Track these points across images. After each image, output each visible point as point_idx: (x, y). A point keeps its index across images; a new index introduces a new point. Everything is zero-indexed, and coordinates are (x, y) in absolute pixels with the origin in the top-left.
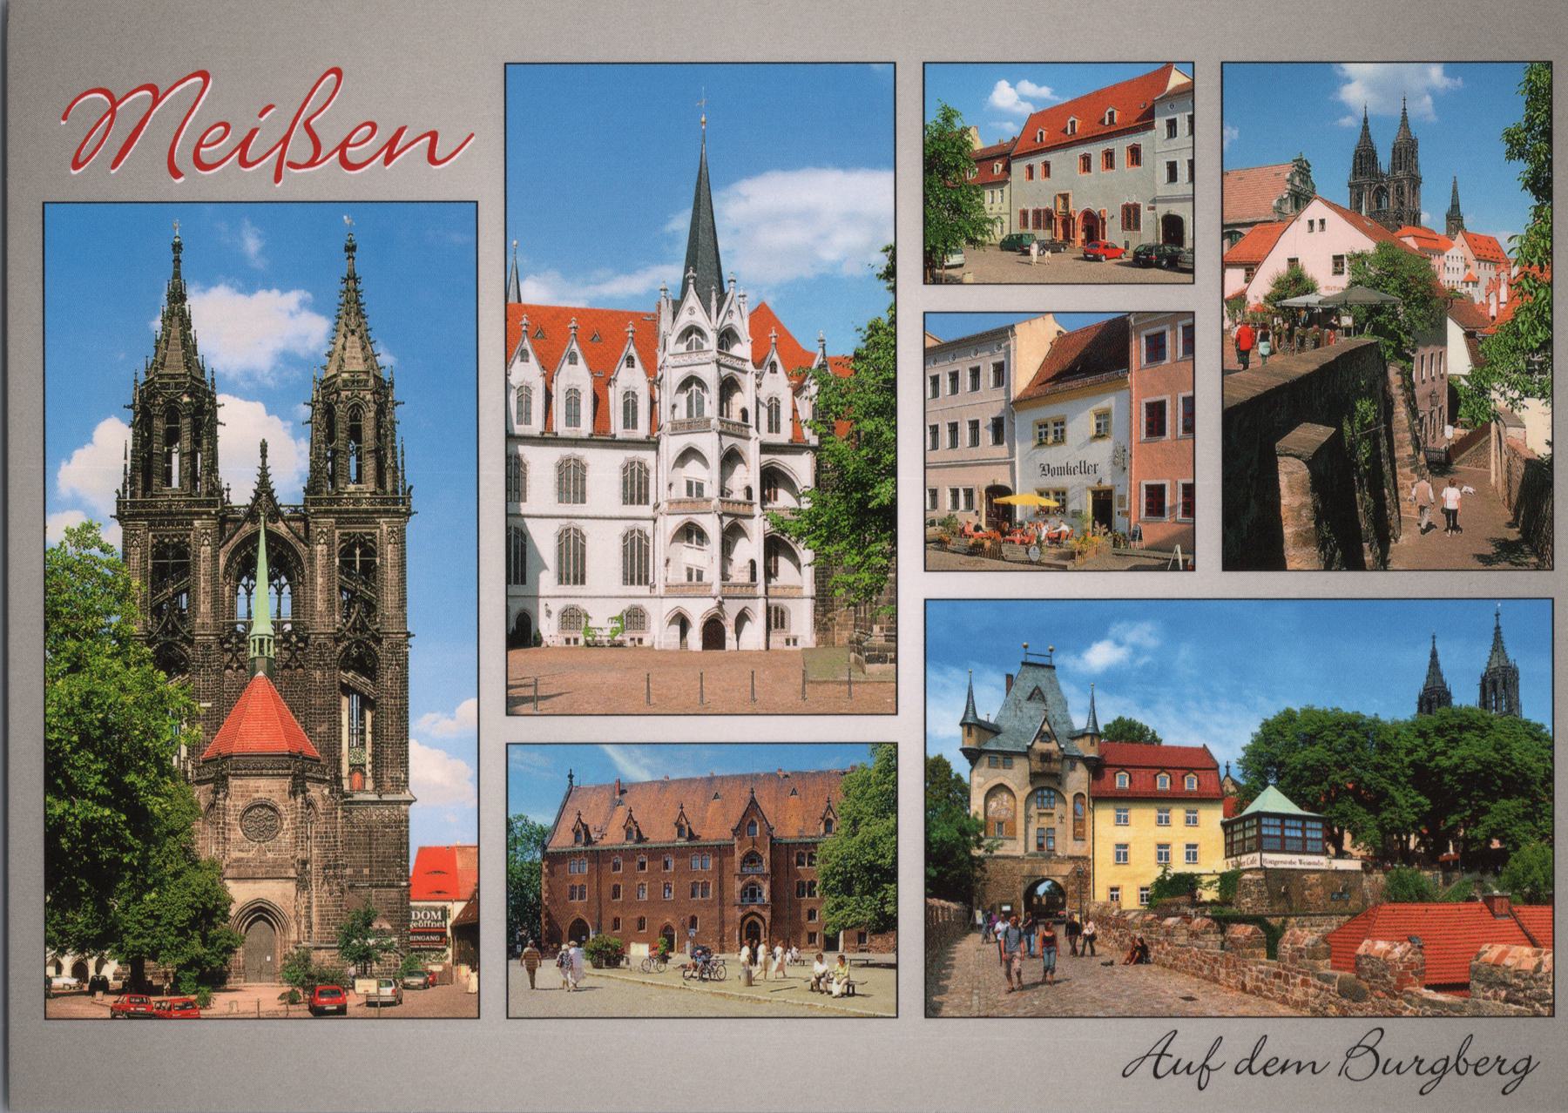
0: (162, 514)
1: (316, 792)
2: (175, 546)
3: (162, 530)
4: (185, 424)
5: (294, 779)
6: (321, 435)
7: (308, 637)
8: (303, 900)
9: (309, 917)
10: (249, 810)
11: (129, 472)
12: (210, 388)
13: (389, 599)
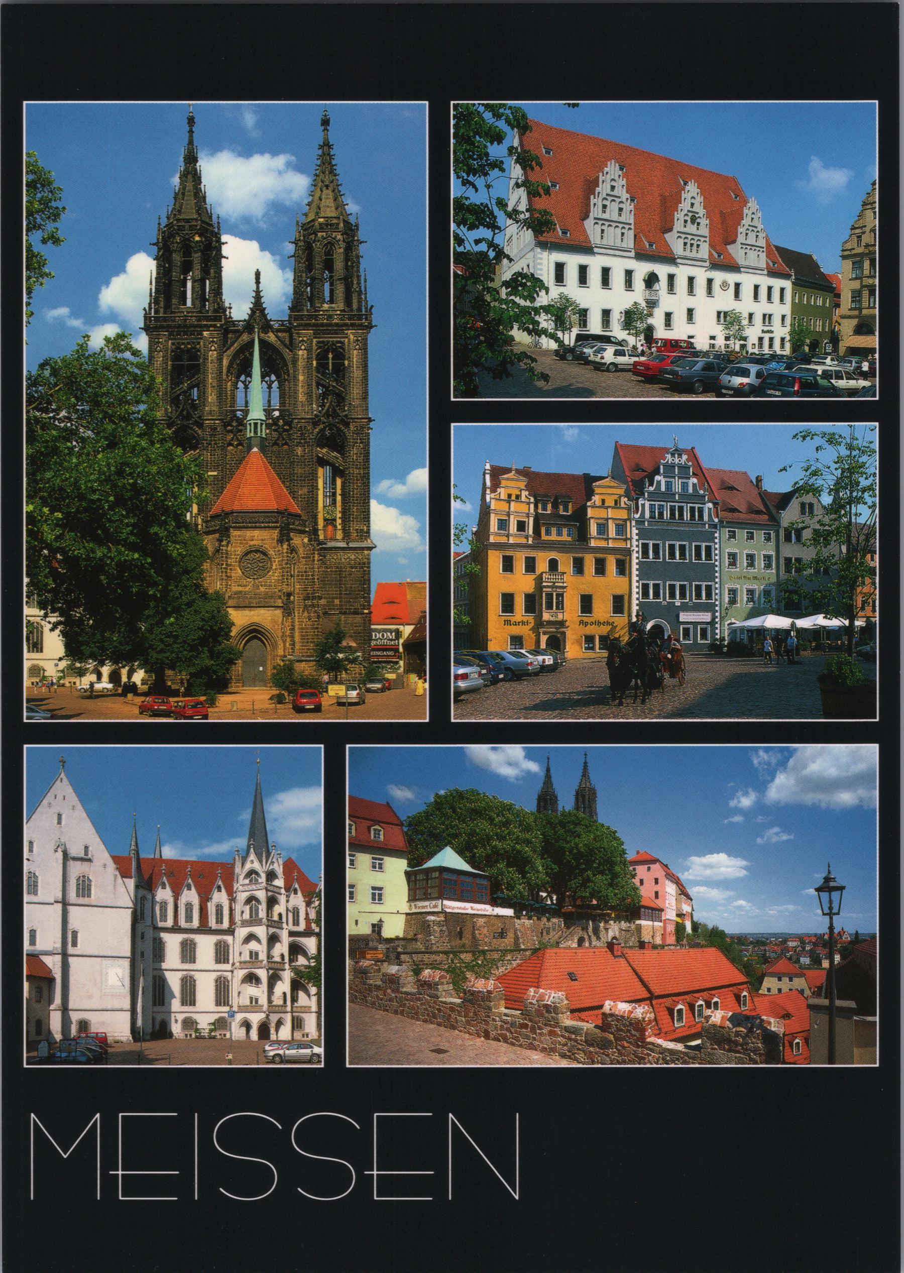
0: (179, 326)
1: (298, 541)
2: (189, 351)
4: (197, 257)
5: (281, 531)
6: (302, 266)
7: (292, 422)
8: (288, 624)
9: (292, 637)
10: (247, 554)
12: (216, 230)
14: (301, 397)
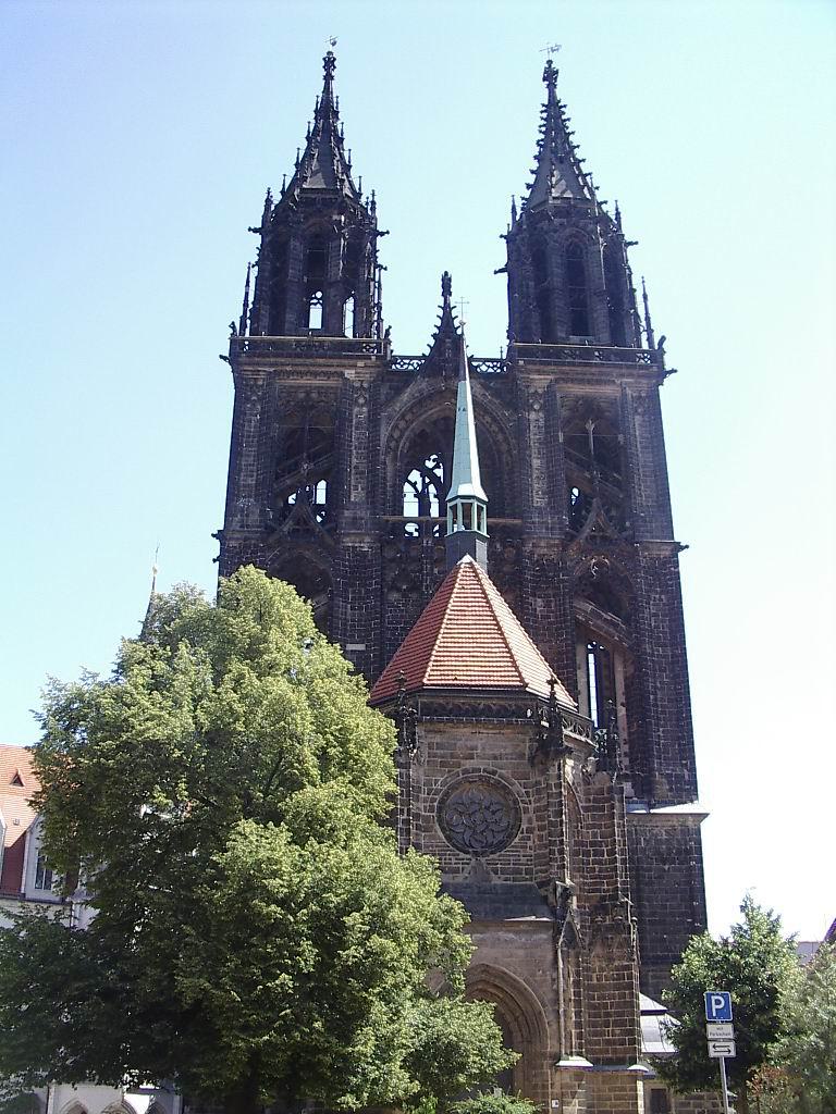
11: (250, 303)
13: (643, 495)
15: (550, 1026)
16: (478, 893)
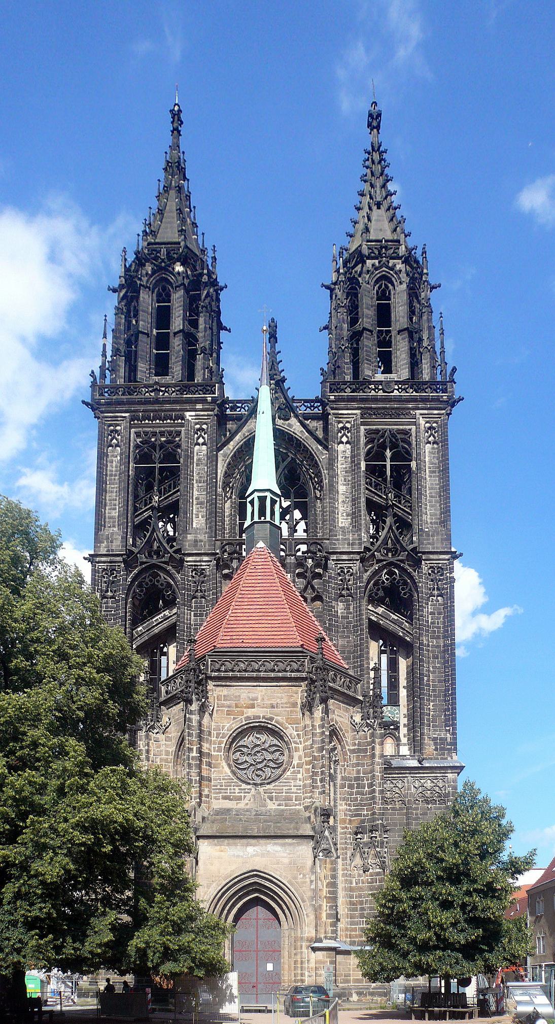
2: (162, 446)
3: (147, 426)
9: (333, 898)
14: (343, 521)
15: (308, 916)
16: (256, 815)
